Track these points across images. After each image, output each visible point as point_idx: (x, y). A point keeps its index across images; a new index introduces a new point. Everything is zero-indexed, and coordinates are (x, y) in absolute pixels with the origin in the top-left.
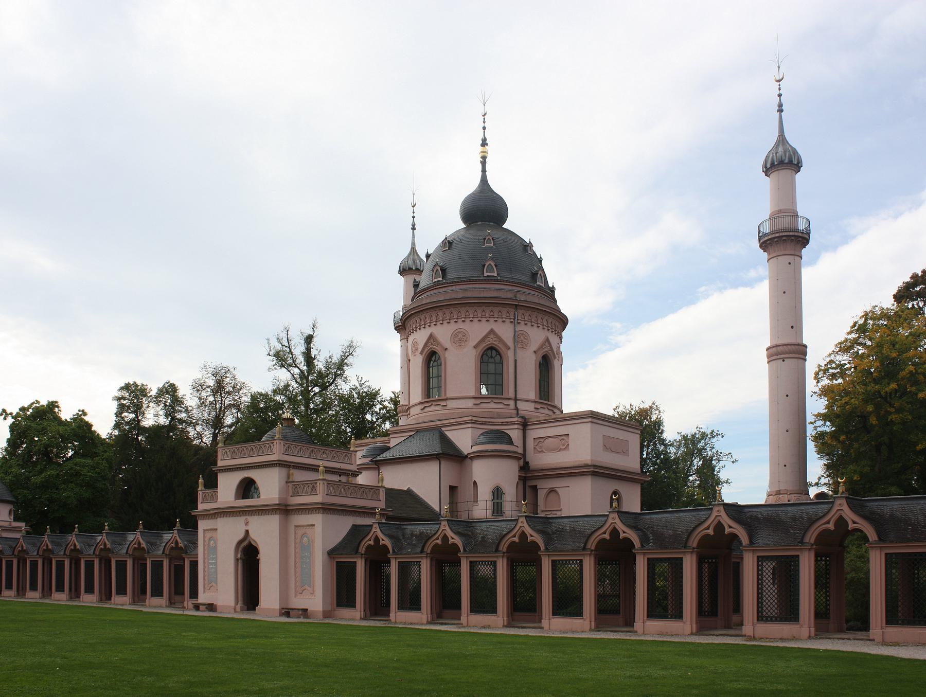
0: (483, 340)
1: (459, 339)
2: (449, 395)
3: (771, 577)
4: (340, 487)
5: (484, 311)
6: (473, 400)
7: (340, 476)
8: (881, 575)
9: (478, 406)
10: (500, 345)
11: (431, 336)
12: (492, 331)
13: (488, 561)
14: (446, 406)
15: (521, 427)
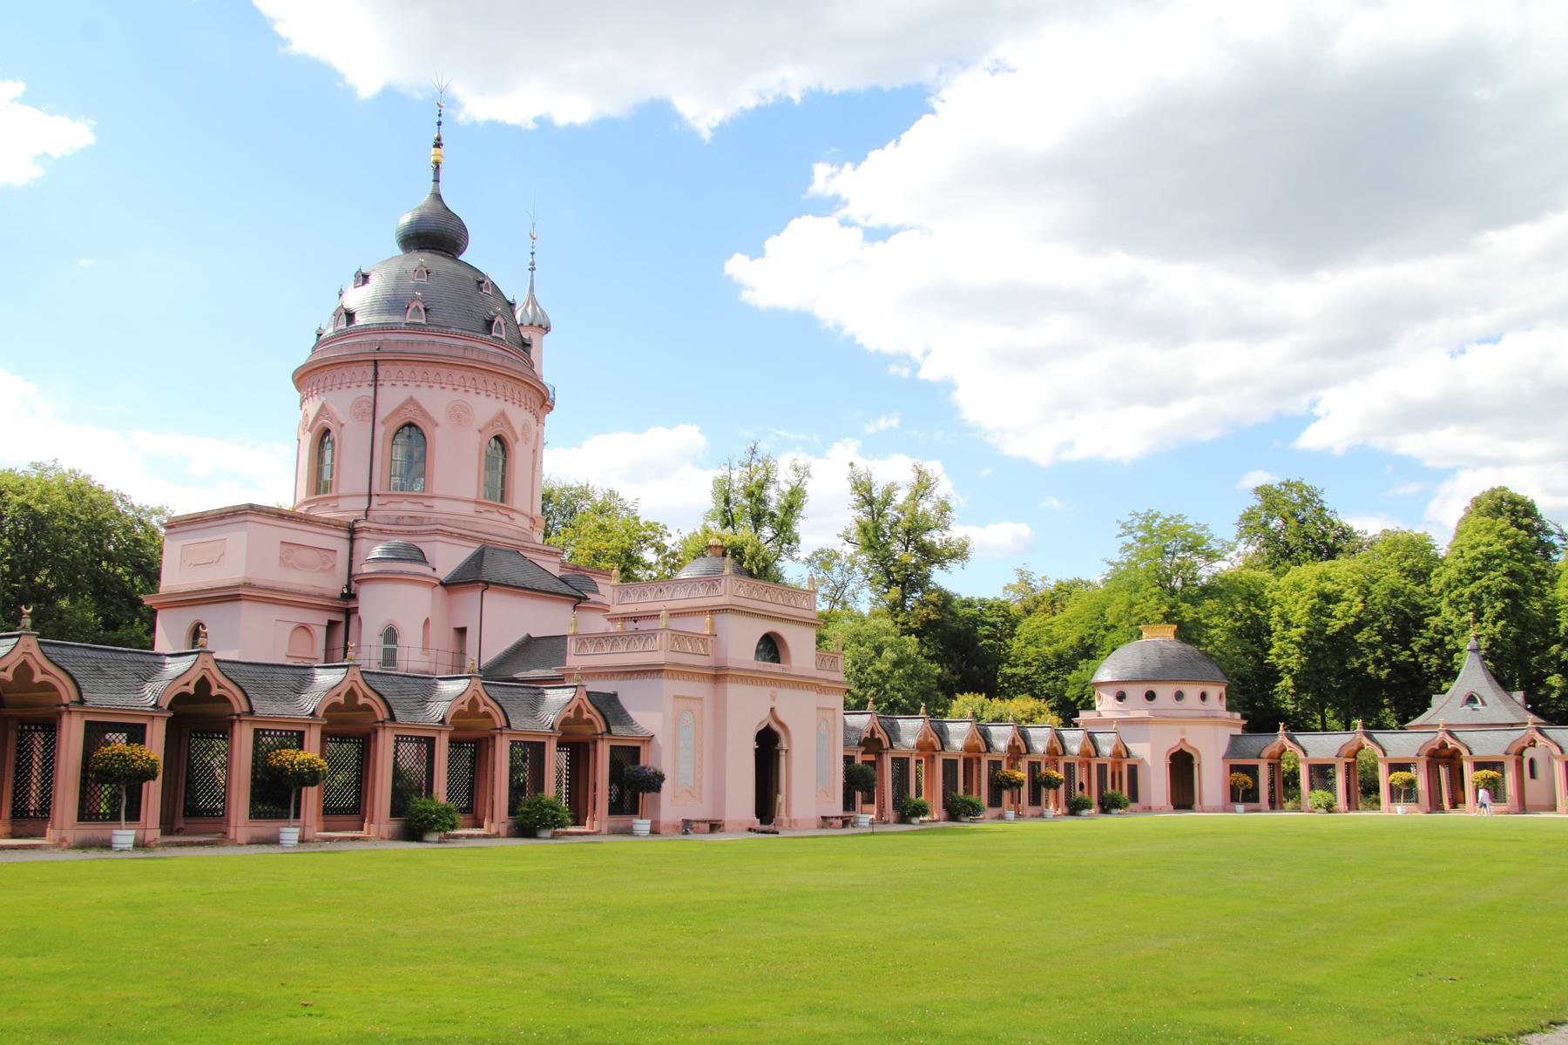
0: (492, 423)
1: (460, 415)
2: (437, 491)
3: (117, 734)
4: (686, 640)
5: (413, 372)
6: (474, 505)
7: (635, 622)
8: (152, 740)
9: (479, 515)
10: (509, 434)
11: (411, 401)
12: (503, 414)
13: (412, 737)
14: (432, 507)
15: (347, 535)
